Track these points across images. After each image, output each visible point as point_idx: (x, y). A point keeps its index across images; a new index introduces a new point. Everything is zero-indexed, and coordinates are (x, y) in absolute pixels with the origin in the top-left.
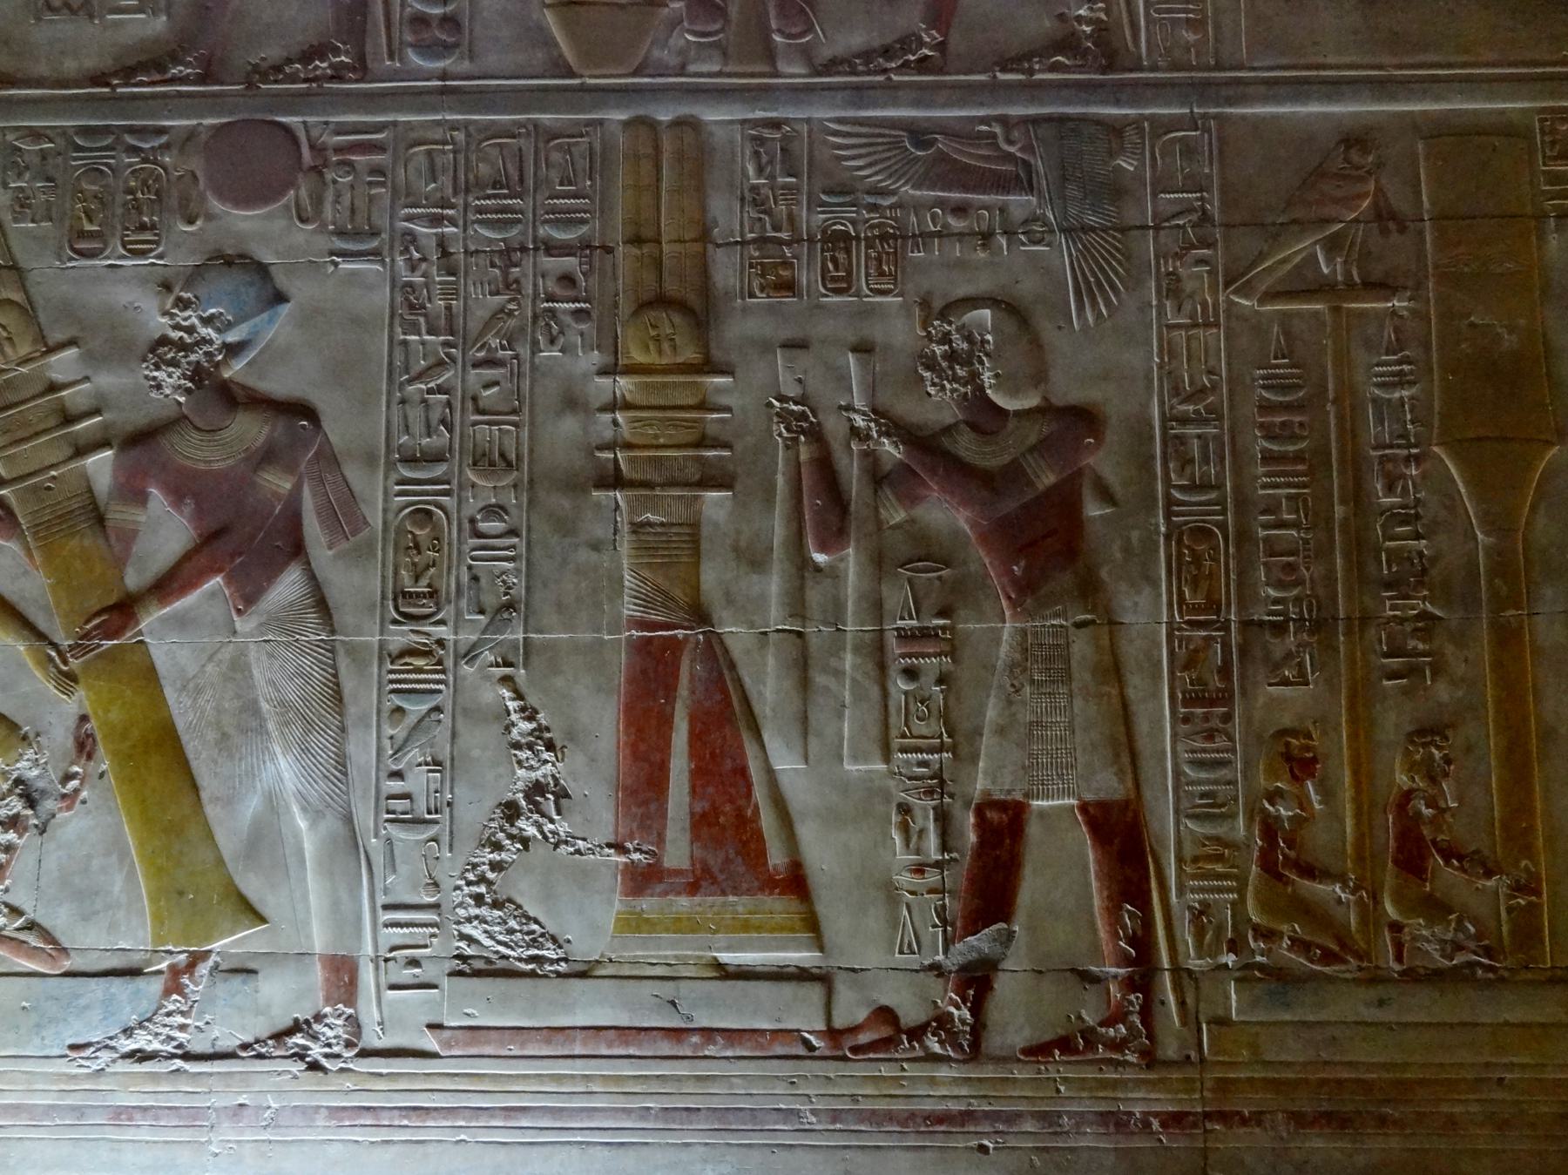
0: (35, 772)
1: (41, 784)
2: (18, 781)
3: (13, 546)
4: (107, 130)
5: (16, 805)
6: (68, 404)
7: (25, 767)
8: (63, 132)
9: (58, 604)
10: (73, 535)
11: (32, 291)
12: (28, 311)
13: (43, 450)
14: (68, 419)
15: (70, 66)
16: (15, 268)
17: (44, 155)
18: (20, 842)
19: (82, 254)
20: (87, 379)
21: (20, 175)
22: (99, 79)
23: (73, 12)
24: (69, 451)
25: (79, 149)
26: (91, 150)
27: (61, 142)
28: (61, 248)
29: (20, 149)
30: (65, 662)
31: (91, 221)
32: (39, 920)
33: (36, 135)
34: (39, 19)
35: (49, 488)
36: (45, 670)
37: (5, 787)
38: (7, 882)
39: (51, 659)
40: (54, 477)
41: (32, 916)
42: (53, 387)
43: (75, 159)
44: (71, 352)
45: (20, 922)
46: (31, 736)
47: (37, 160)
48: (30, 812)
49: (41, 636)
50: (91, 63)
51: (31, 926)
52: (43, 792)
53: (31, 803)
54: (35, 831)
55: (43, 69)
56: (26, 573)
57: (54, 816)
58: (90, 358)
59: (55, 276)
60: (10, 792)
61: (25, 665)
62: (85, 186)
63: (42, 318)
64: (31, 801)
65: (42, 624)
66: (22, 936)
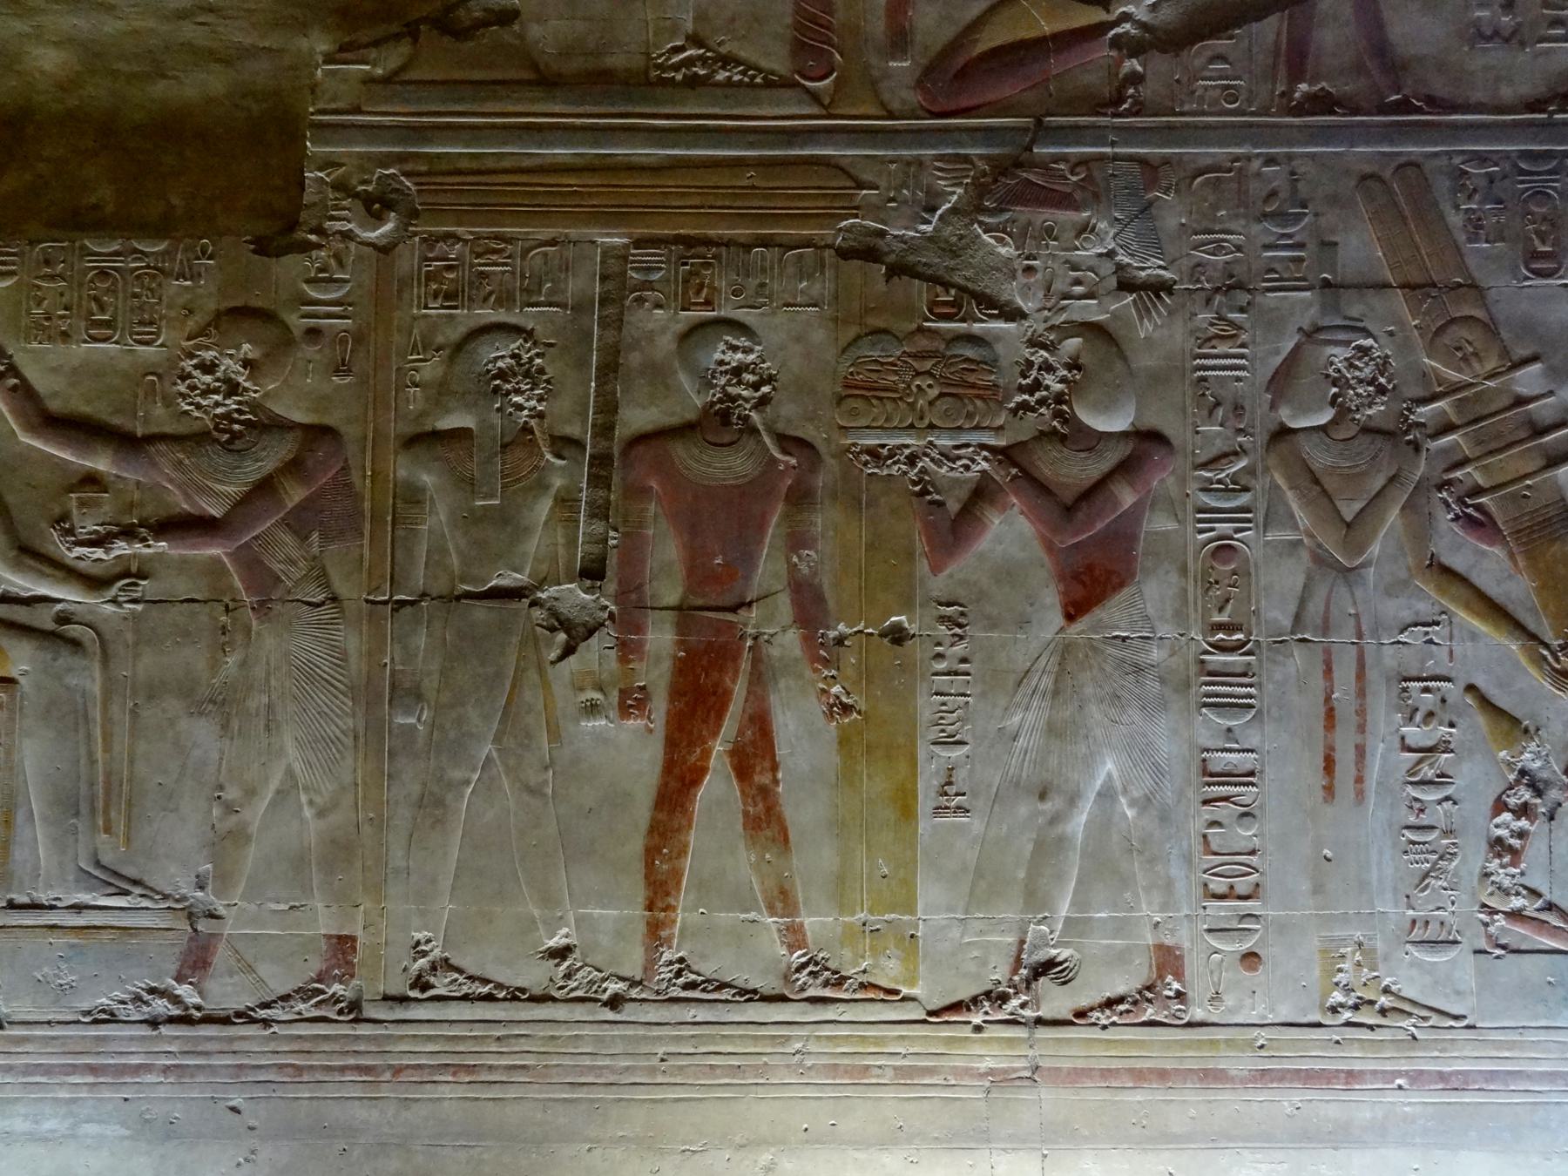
0: (1538, 764)
1: (1545, 775)
2: (1523, 772)
3: (1497, 551)
4: (1547, 155)
5: (1526, 795)
6: (1534, 417)
7: (1528, 759)
8: (1506, 155)
9: (1545, 607)
10: (1554, 540)
11: (1494, 310)
12: (1490, 329)
13: (1512, 462)
14: (1539, 431)
15: (1506, 93)
16: (1474, 286)
17: (1491, 178)
18: (1532, 829)
19: (1539, 274)
20: (1551, 393)
21: (1470, 197)
22: (1534, 105)
23: (1507, 40)
24: (1540, 462)
25: (1522, 172)
26: (1539, 173)
27: (1507, 166)
28: (1517, 267)
29: (1466, 173)
30: (1557, 660)
31: (1544, 242)
32: (1556, 899)
33: (1482, 159)
34: (1472, 48)
35: (1525, 496)
36: (1541, 668)
37: (1512, 777)
38: (1523, 866)
39: (1545, 658)
40: (1529, 487)
41: (1548, 897)
42: (1521, 401)
43: (1522, 182)
44: (1536, 368)
45: (1539, 903)
46: (1532, 729)
47: (1483, 183)
48: (1538, 801)
49: (1533, 637)
50: (1526, 88)
51: (1550, 907)
52: (1547, 783)
53: (1539, 793)
54: (1543, 818)
55: (1478, 96)
56: (1510, 576)
57: (1560, 805)
58: (1553, 373)
59: (1515, 295)
60: (1518, 782)
61: (1518, 662)
62: (1536, 209)
63: (1504, 334)
64: (1538, 789)
65: (1532, 626)
66: (1543, 916)
